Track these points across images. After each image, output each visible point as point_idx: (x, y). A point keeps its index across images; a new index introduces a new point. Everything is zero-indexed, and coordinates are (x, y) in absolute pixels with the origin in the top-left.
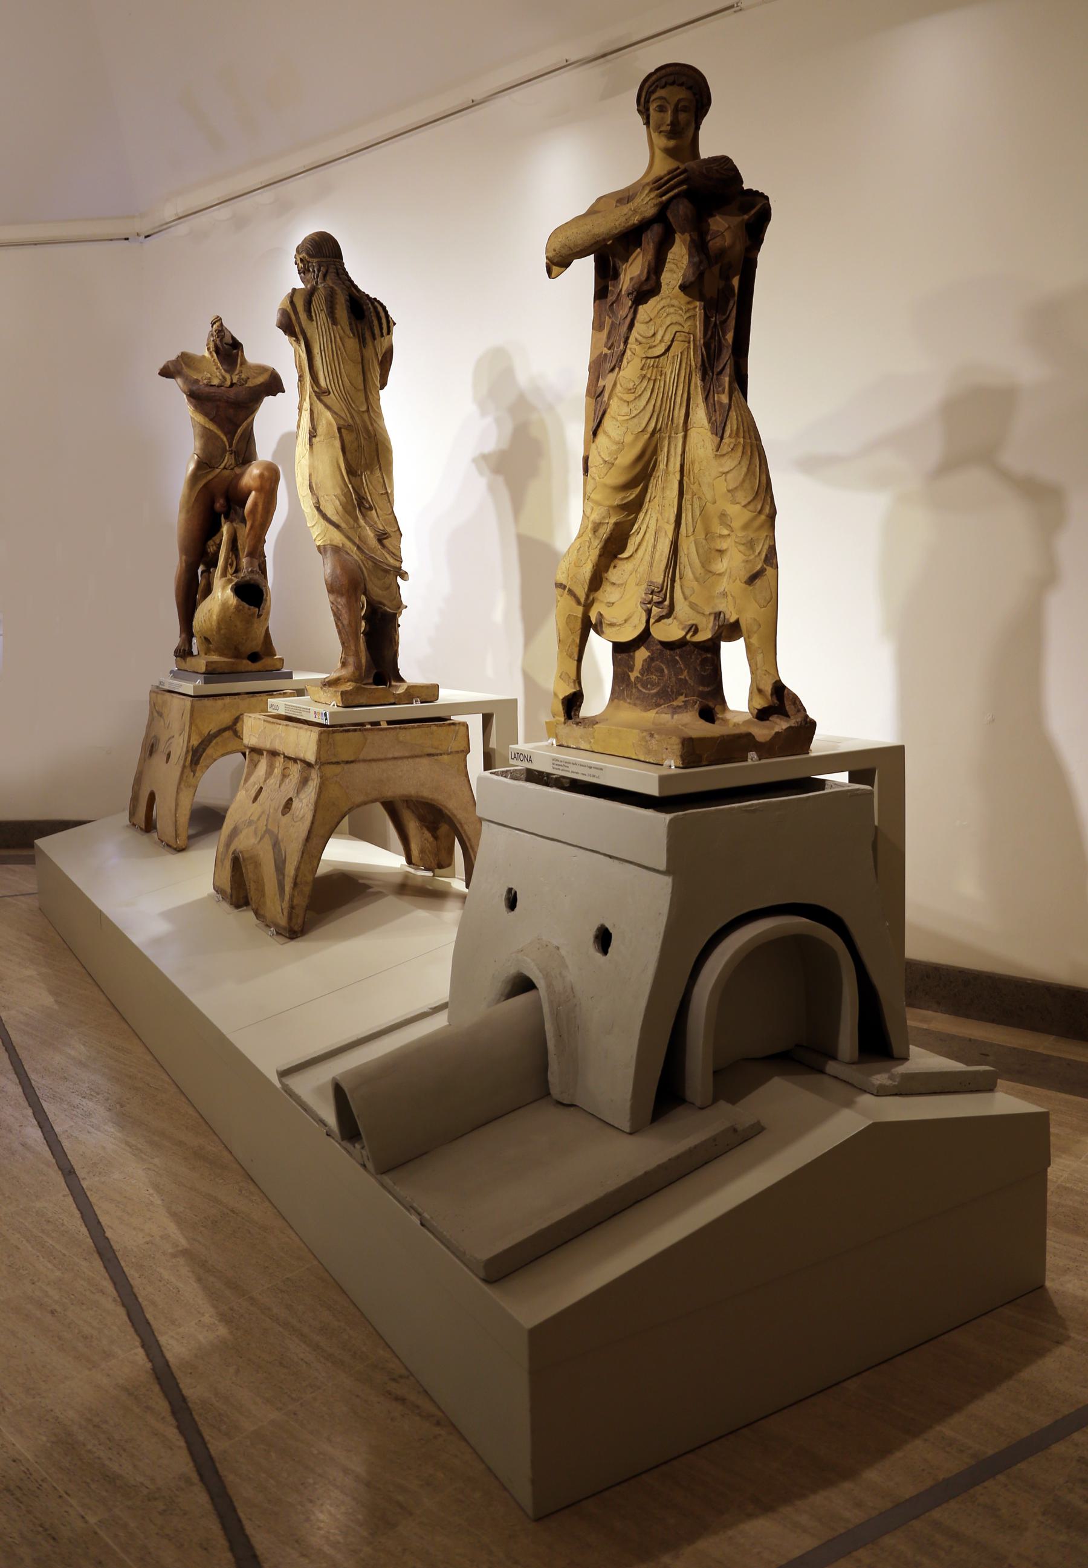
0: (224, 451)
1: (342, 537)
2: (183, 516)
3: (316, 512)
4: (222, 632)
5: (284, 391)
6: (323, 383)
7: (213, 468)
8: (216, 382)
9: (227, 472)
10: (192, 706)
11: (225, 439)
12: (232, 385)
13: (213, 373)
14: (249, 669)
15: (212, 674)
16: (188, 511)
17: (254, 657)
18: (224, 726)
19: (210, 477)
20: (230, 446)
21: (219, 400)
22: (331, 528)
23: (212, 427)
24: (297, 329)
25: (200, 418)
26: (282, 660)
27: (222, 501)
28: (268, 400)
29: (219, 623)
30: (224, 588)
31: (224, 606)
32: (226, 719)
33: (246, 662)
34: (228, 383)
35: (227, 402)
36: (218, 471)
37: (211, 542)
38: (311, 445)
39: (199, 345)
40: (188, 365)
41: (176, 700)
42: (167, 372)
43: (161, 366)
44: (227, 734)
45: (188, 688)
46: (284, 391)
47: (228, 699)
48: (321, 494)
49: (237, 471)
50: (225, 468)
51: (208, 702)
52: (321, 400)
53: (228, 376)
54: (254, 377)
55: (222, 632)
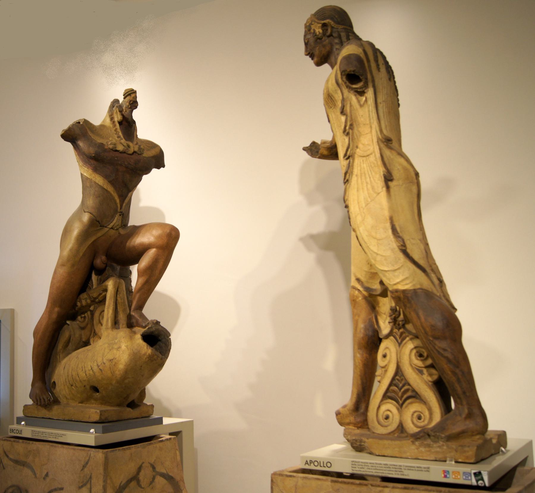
0: (116, 211)
1: (429, 282)
2: (62, 271)
3: (401, 256)
4: (126, 381)
5: (164, 166)
6: (385, 132)
7: (103, 226)
8: (120, 148)
9: (112, 232)
10: (106, 458)
11: (118, 201)
12: (135, 152)
13: (115, 140)
14: (130, 416)
15: (105, 423)
16: (73, 266)
17: (133, 405)
18: (130, 477)
19: (99, 234)
20: (121, 209)
21: (121, 165)
22: (419, 272)
23: (110, 189)
24: (369, 77)
25: (99, 180)
26: (152, 406)
27: (104, 258)
28: (154, 171)
29: (126, 372)
30: (131, 338)
31: (135, 356)
32: (132, 468)
33: (129, 409)
34: (131, 151)
35: (127, 167)
36: (106, 229)
37: (84, 296)
38: (388, 188)
39: (99, 116)
40: (92, 132)
41: (61, 451)
42: (69, 136)
43: (66, 127)
44: (133, 484)
45: (90, 437)
46: (164, 166)
47: (134, 448)
48: (406, 237)
49: (122, 232)
50: (112, 228)
51: (118, 452)
52: (390, 148)
53: (131, 144)
54: (148, 150)
55: (126, 381)
